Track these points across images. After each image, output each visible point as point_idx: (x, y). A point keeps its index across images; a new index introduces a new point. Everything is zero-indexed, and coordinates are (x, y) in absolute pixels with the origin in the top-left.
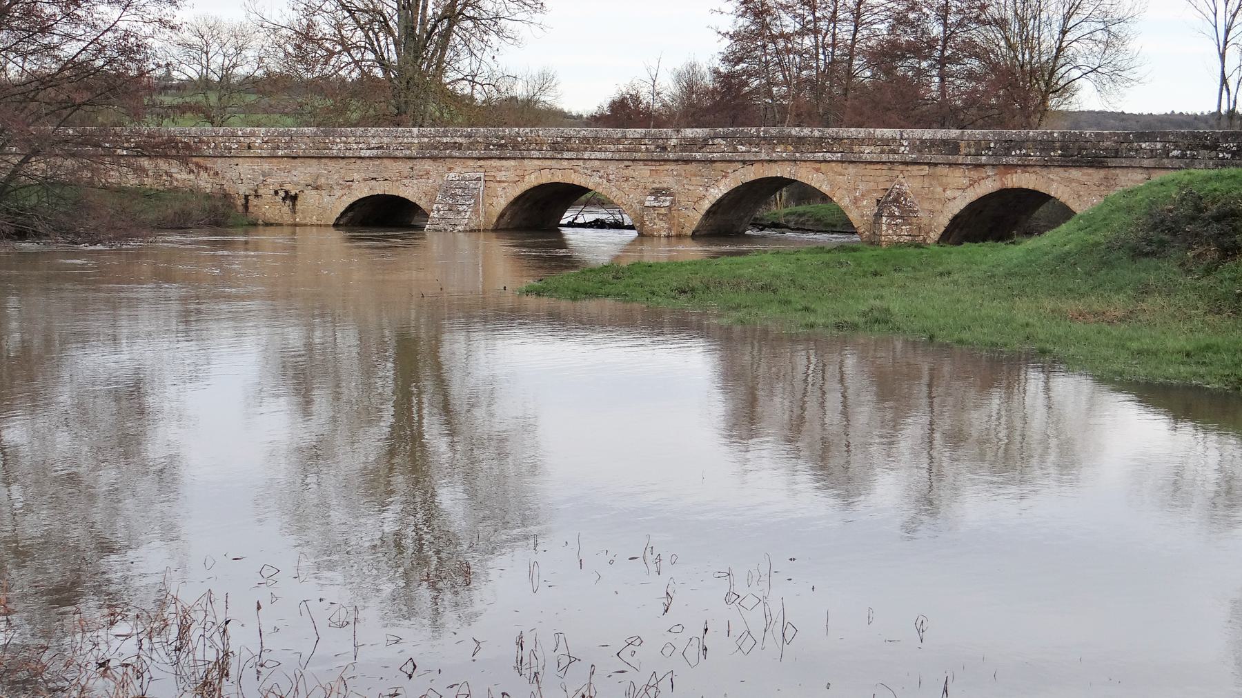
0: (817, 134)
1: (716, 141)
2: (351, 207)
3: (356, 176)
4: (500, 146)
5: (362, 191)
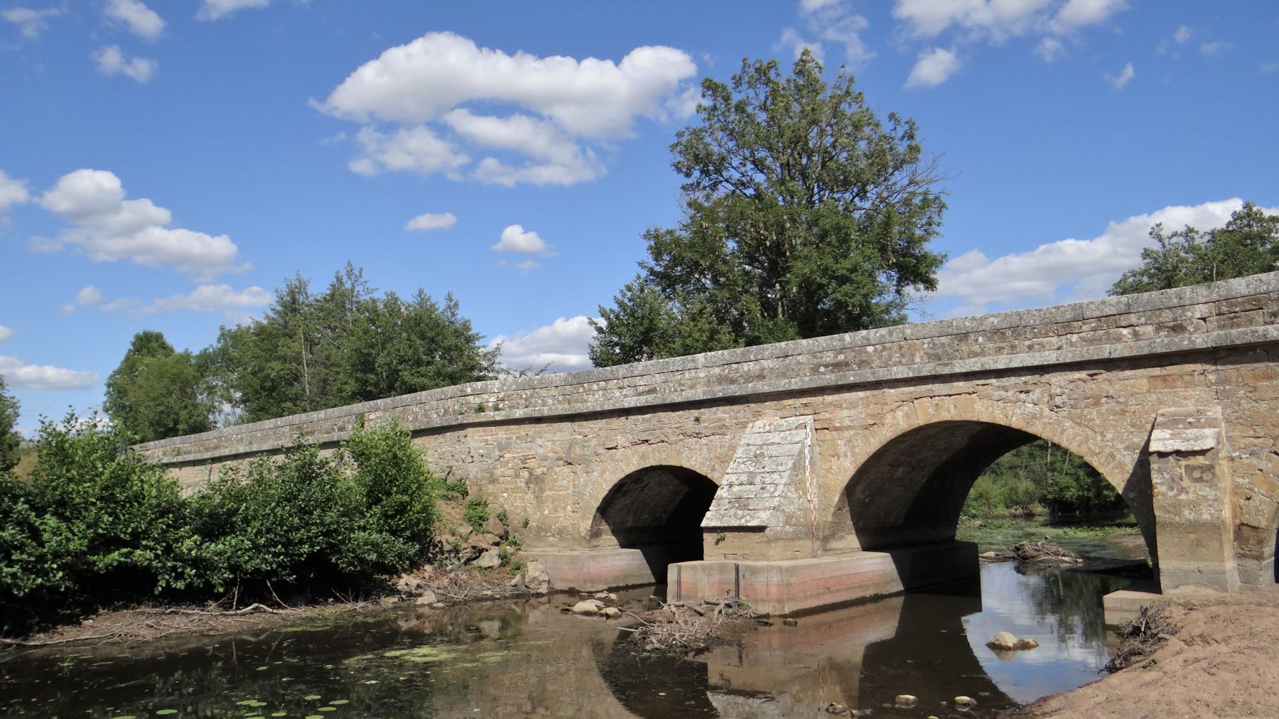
2: (620, 489)
3: (620, 440)
4: (837, 366)
5: (630, 463)
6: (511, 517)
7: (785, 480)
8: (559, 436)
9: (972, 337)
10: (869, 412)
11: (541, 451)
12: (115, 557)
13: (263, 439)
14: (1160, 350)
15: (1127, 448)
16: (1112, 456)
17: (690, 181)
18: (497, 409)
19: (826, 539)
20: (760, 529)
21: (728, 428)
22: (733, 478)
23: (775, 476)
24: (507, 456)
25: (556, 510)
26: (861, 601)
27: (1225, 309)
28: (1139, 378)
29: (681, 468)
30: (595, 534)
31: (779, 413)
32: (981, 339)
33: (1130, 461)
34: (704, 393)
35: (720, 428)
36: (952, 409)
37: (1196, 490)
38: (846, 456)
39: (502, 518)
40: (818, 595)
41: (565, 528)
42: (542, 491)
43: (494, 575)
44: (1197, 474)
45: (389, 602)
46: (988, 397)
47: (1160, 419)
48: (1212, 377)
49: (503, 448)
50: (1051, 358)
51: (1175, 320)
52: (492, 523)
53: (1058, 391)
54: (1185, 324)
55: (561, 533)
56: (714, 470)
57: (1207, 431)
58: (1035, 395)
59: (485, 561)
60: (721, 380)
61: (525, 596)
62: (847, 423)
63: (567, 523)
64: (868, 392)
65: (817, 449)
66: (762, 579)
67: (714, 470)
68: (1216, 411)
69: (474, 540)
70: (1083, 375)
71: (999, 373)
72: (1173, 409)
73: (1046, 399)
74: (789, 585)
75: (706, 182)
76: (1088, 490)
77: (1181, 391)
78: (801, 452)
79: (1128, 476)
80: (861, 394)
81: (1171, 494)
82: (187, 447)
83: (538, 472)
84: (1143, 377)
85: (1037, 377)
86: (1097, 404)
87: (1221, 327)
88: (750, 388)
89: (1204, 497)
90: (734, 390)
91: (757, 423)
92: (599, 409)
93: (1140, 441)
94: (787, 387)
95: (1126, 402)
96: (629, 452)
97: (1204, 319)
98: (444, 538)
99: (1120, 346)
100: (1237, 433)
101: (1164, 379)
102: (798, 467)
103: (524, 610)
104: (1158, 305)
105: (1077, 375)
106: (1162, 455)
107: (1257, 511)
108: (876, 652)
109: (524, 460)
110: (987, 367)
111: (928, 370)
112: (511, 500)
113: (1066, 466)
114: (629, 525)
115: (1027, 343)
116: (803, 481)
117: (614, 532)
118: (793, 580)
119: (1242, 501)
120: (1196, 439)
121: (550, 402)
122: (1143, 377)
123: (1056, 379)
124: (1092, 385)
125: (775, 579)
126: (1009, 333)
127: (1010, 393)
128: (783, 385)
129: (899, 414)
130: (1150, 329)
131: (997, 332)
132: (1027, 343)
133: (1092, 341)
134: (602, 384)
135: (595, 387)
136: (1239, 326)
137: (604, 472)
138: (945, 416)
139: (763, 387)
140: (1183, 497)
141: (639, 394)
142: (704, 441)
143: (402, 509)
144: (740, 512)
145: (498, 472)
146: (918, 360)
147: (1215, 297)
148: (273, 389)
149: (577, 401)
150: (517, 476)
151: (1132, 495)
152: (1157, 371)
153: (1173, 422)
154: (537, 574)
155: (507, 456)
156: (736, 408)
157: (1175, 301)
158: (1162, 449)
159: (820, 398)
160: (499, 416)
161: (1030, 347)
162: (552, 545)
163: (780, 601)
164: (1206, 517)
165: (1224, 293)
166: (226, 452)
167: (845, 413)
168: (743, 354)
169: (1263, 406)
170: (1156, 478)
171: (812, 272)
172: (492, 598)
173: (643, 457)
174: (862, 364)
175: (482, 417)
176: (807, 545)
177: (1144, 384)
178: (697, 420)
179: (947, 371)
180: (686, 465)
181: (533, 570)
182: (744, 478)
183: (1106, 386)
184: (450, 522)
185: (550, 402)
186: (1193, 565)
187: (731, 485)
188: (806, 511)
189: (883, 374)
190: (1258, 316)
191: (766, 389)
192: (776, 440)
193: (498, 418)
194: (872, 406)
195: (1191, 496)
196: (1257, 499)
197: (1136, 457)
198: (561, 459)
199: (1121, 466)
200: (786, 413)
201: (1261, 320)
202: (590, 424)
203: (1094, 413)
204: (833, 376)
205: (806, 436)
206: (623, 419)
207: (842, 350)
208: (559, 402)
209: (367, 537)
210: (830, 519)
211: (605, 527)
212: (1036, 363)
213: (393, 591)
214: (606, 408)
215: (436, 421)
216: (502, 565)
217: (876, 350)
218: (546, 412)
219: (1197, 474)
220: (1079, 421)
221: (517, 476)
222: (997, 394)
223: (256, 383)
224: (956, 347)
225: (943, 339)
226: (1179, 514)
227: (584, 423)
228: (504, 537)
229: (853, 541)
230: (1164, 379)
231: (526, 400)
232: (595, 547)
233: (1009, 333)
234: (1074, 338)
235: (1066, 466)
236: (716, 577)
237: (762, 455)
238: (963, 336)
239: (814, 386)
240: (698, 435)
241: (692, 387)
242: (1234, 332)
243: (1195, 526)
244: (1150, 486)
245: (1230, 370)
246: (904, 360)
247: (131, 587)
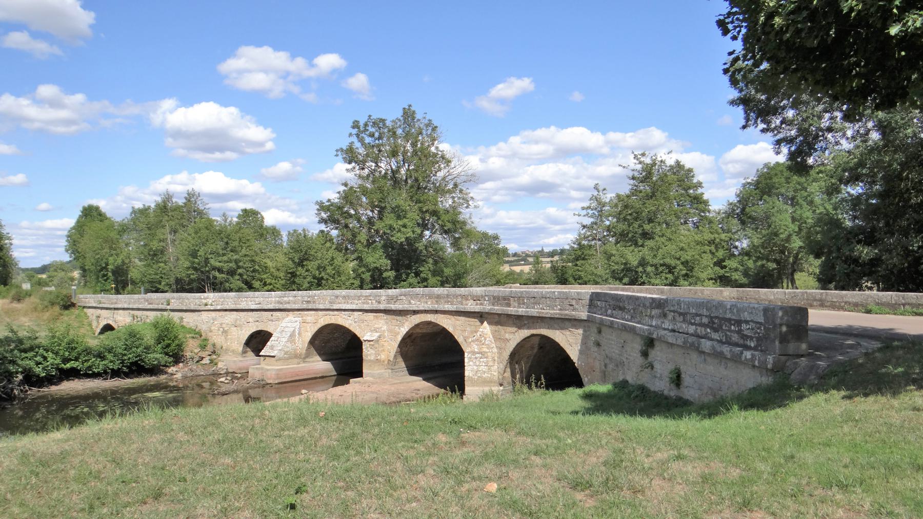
0: (446, 292)
3: (251, 320)
4: (308, 302)
12: (68, 366)
13: (135, 303)
26: (316, 378)
30: (244, 352)
39: (214, 345)
49: (214, 319)
50: (354, 307)
52: (210, 348)
55: (233, 351)
59: (203, 362)
60: (279, 302)
61: (217, 375)
71: (345, 310)
82: (103, 300)
90: (281, 307)
98: (188, 354)
109: (221, 324)
112: (217, 338)
123: (356, 313)
143: (168, 346)
148: (155, 255)
166: (120, 306)
174: (314, 302)
175: (207, 308)
176: (296, 360)
181: (220, 365)
184: (191, 348)
209: (156, 357)
211: (248, 349)
213: (166, 373)
215: (192, 307)
223: (146, 252)
228: (214, 352)
245: (389, 317)
247: (73, 374)
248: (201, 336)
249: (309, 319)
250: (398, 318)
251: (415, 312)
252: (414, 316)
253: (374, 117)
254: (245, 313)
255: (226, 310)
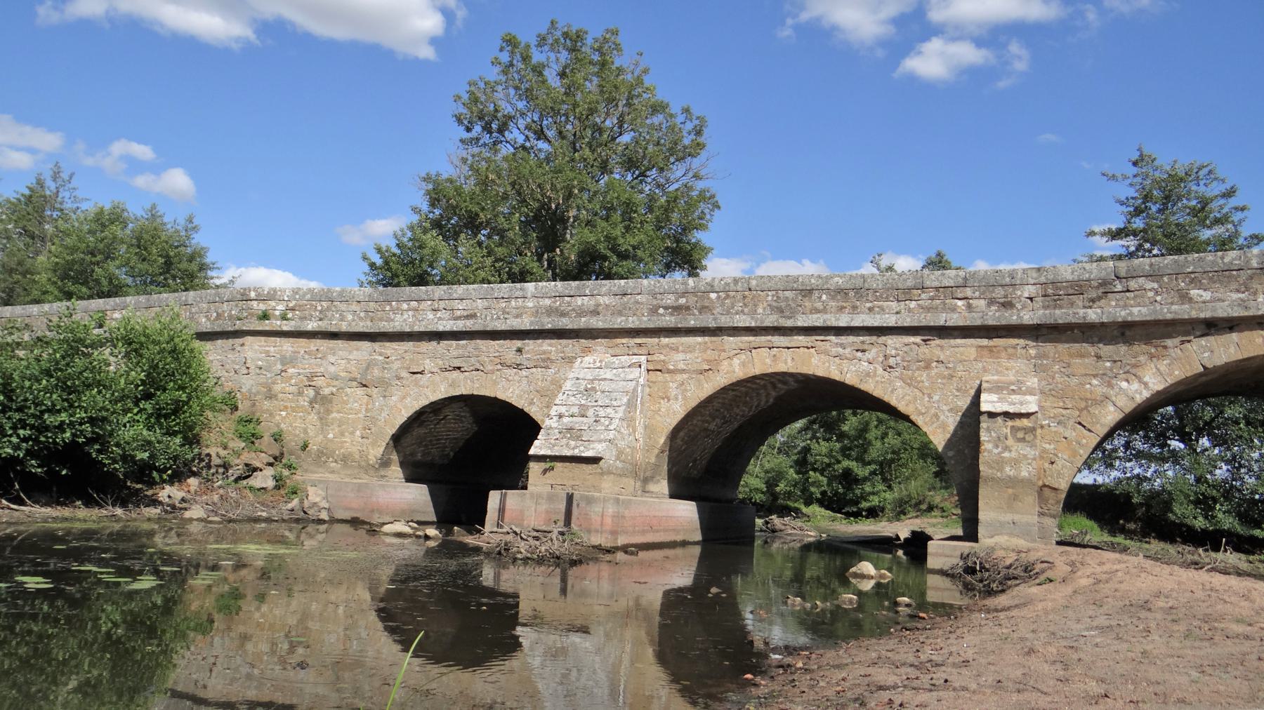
1: (1133, 284)
2: (419, 418)
3: (428, 365)
4: (677, 309)
6: (287, 438)
7: (620, 414)
8: (355, 355)
9: (816, 294)
10: (705, 356)
11: (332, 369)
14: (991, 322)
15: (951, 410)
16: (936, 416)
17: (469, 135)
18: (284, 318)
19: (646, 481)
20: (595, 460)
21: (552, 361)
22: (563, 410)
23: (609, 410)
24: (291, 371)
25: (342, 434)
27: (1050, 291)
28: (968, 347)
29: (495, 401)
30: (385, 463)
31: (610, 351)
32: (824, 297)
33: (952, 422)
34: (531, 323)
35: (543, 360)
36: (789, 361)
37: (1018, 450)
38: (677, 399)
39: (277, 438)
40: (643, 532)
41: (350, 454)
42: (328, 412)
43: (267, 497)
44: (1020, 435)
45: (154, 512)
46: (827, 353)
47: (984, 385)
48: (1032, 352)
50: (891, 321)
51: (1006, 297)
53: (893, 352)
54: (1014, 301)
55: (345, 459)
56: (532, 403)
57: (1029, 398)
58: (868, 355)
59: (258, 481)
60: (550, 311)
61: (303, 520)
62: (681, 366)
63: (354, 449)
64: (707, 338)
65: (648, 390)
66: (597, 509)
67: (532, 403)
68: (1033, 382)
69: (248, 457)
70: (918, 339)
72: (995, 378)
73: (880, 359)
74: (623, 517)
75: (486, 138)
76: (795, 486)
77: (1004, 362)
78: (635, 390)
79: (948, 436)
80: (699, 339)
81: (996, 451)
83: (326, 391)
84: (972, 345)
85: (874, 338)
86: (928, 367)
87: (1045, 307)
88: (583, 323)
89: (1025, 456)
91: (586, 359)
92: (407, 329)
93: (964, 403)
94: (623, 325)
95: (955, 368)
96: (437, 378)
97: (1031, 299)
99: (955, 316)
100: (1048, 404)
101: (990, 349)
102: (631, 405)
103: (298, 537)
104: (992, 282)
105: (912, 339)
106: (992, 415)
107: (1059, 474)
108: (673, 599)
109: (311, 377)
110: (829, 324)
111: (770, 321)
112: (291, 419)
113: (757, 469)
114: (419, 457)
115: (868, 305)
116: (633, 419)
117: (402, 464)
118: (627, 513)
119: (1047, 465)
120: (1021, 403)
121: (350, 317)
122: (972, 345)
123: (892, 341)
124: (924, 350)
125: (611, 510)
126: (852, 294)
127: (848, 350)
128: (619, 322)
129: (736, 361)
130: (982, 303)
131: (841, 292)
132: (868, 305)
133: (928, 309)
134: (414, 304)
135: (405, 306)
136: (1061, 307)
137: (404, 397)
138: (781, 368)
139: (597, 323)
140: (1006, 454)
141: (456, 319)
142: (524, 373)
143: (178, 408)
144: (572, 443)
145: (277, 388)
146: (760, 310)
147: (1043, 279)
149: (381, 320)
150: (300, 393)
151: (950, 454)
152: (985, 342)
153: (998, 388)
154: (318, 500)
155: (291, 371)
156: (564, 342)
157: (1008, 280)
158: (993, 410)
159: (656, 340)
160: (286, 327)
161: (870, 309)
162: (333, 472)
163: (614, 533)
164: (1024, 474)
165: (1051, 277)
167: (681, 356)
168: (578, 288)
169: (1075, 381)
170: (984, 436)
171: (598, 241)
172: (268, 520)
173: (453, 385)
174: (703, 309)
175: (267, 326)
177: (972, 353)
178: (519, 350)
179: (789, 323)
180: (501, 396)
182: (575, 410)
183: (937, 352)
185: (350, 317)
186: (1008, 517)
187: (560, 416)
188: (633, 448)
189: (725, 321)
190: (1079, 301)
191: (601, 325)
192: (608, 376)
193: (285, 328)
194: (709, 352)
195: (1014, 454)
196: (1060, 463)
197: (958, 418)
198: (354, 379)
199: (944, 426)
200: (618, 351)
201: (1080, 304)
202: (395, 345)
203: (923, 376)
204: (673, 319)
205: (639, 375)
206: (434, 343)
207: (684, 294)
208: (361, 319)
209: (133, 432)
210: (653, 460)
211: (395, 457)
212: (876, 324)
213: (154, 502)
214: (416, 329)
216: (277, 487)
217: (719, 297)
218: (344, 327)
219: (1020, 435)
220: (910, 382)
221: (300, 393)
222: (834, 351)
224: (799, 302)
225: (788, 294)
226: (1001, 470)
227: (388, 344)
229: (663, 486)
230: (990, 349)
231: (321, 312)
232: (383, 477)
233: (852, 294)
234: (913, 305)
235: (757, 469)
236: (544, 507)
237: (593, 389)
238: (808, 292)
239: (652, 326)
240: (518, 366)
241: (517, 317)
242: (1057, 312)
243: (1013, 482)
244: (978, 443)
245: (1049, 348)
246: (746, 310)
248: (235, 408)
249: (678, 359)
250: (1105, 350)
251: (1212, 326)
252: (1203, 341)
253: (562, 26)
254: (409, 345)
255: (334, 336)
